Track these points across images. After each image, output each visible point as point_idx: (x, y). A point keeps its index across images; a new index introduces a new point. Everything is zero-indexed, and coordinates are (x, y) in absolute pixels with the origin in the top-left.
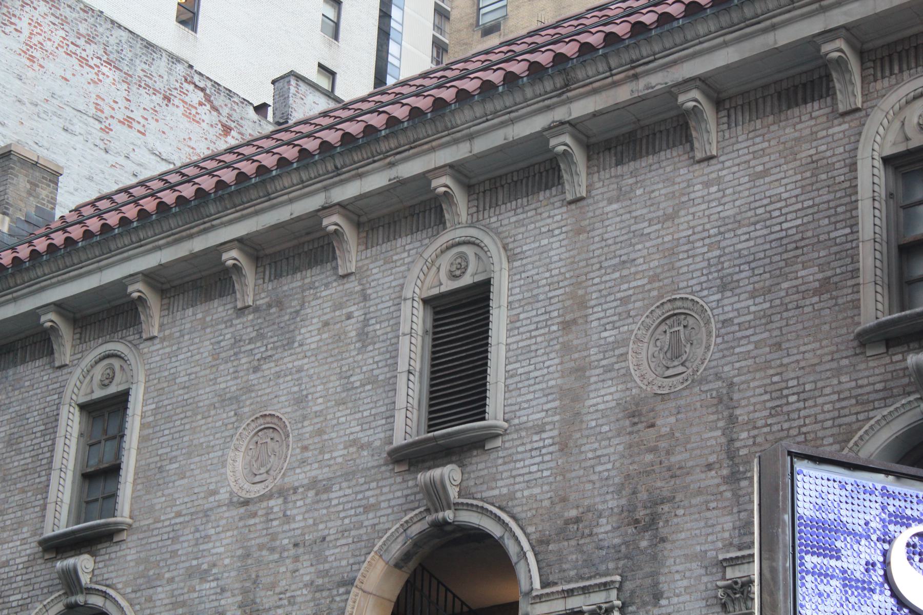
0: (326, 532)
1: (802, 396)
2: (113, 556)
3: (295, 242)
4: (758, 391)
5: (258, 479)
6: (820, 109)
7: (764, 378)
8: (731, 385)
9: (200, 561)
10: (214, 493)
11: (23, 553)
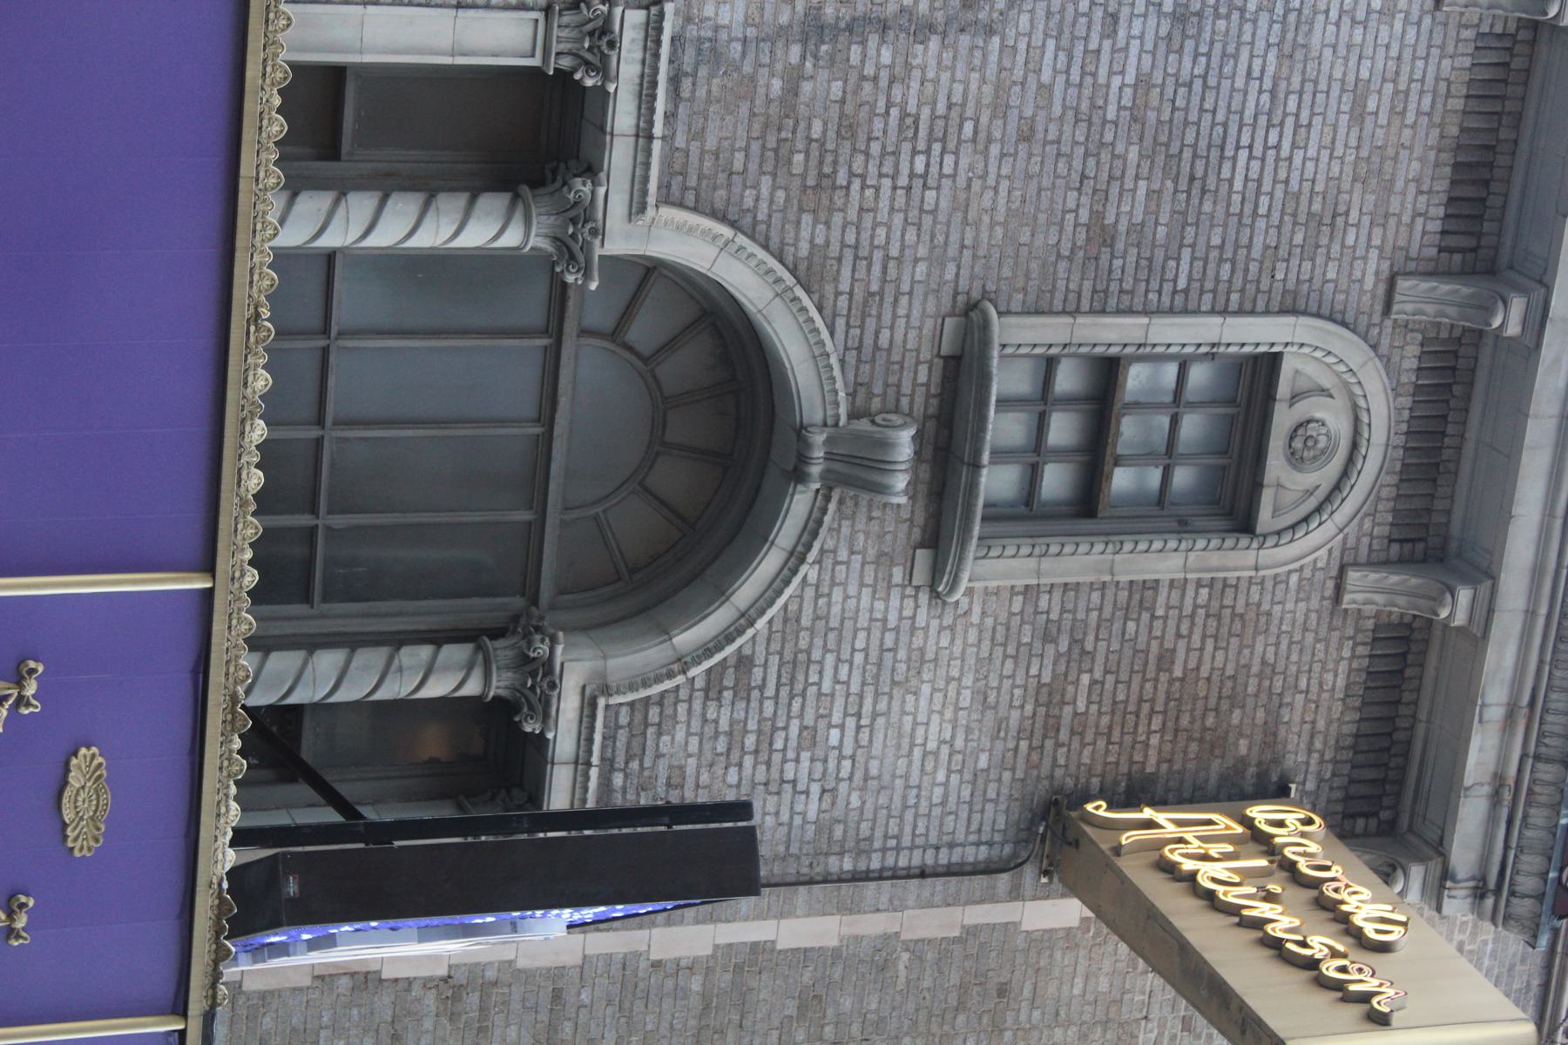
1: (918, 183)
4: (958, 89)
6: (1424, 233)
7: (978, 102)
8: (990, 31)
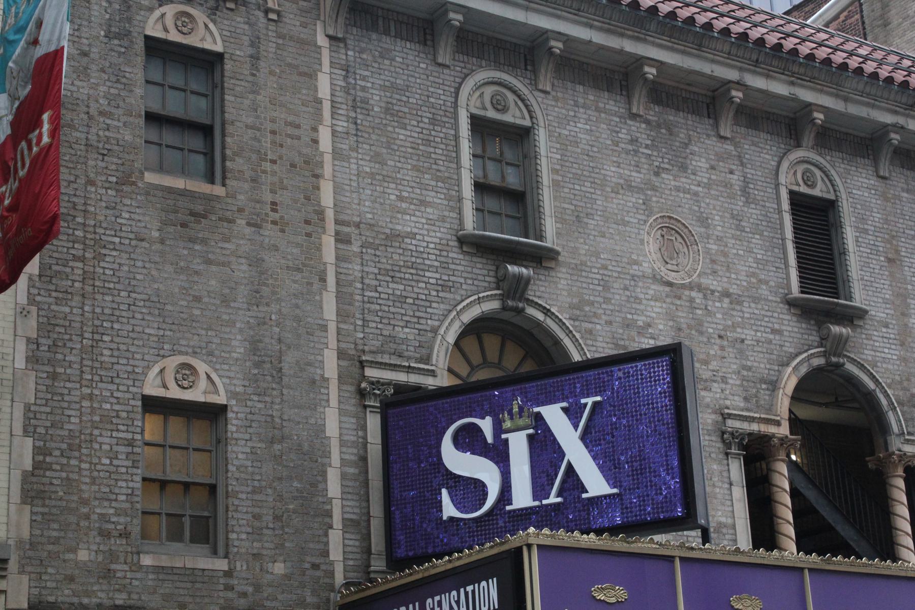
0: (744, 337)
2: (543, 278)
3: (676, 85)
5: (669, 266)
9: (635, 317)
10: (636, 263)
11: (433, 234)
